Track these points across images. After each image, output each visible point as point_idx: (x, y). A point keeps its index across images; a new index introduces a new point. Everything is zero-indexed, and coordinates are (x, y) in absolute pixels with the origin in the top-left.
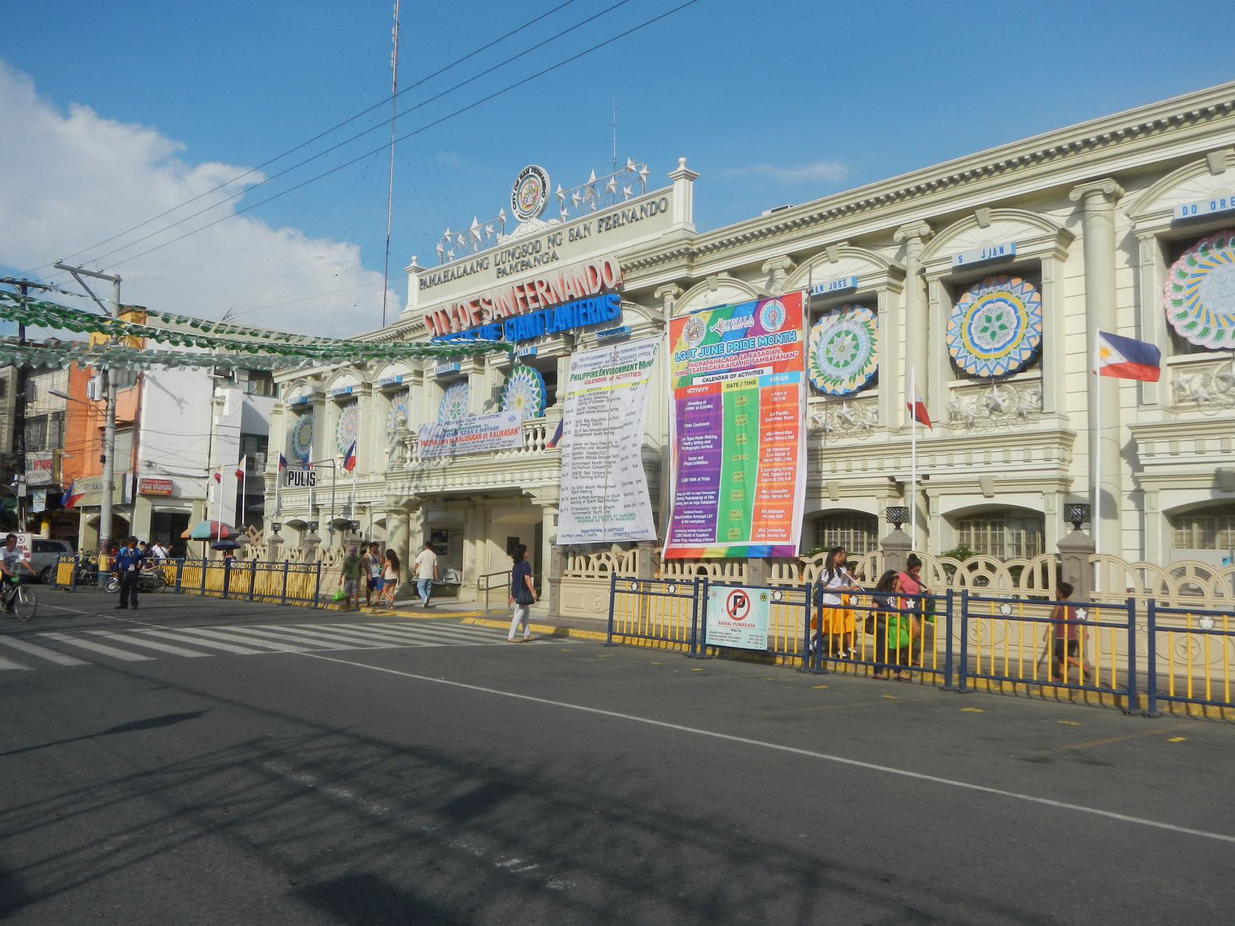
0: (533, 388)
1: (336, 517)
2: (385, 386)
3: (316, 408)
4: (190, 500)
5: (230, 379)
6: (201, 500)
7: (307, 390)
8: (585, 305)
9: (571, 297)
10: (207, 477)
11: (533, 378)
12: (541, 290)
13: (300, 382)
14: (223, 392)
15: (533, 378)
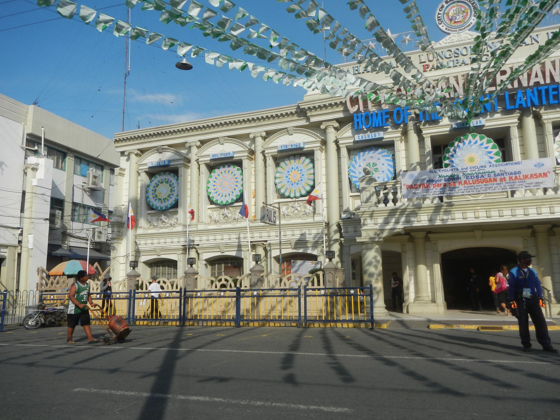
0: (489, 150)
1: (284, 252)
2: (280, 151)
3: (181, 171)
4: (6, 246)
5: (36, 152)
6: (15, 247)
7: (167, 156)
8: (554, 90)
9: (537, 84)
10: (19, 228)
11: (488, 142)
12: (499, 78)
13: (160, 150)
14: (32, 160)
15: (488, 142)
